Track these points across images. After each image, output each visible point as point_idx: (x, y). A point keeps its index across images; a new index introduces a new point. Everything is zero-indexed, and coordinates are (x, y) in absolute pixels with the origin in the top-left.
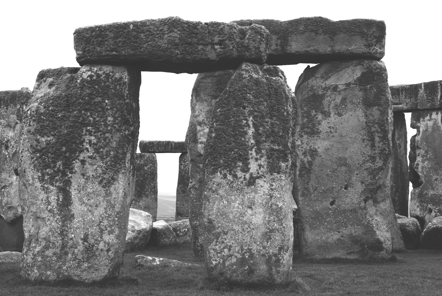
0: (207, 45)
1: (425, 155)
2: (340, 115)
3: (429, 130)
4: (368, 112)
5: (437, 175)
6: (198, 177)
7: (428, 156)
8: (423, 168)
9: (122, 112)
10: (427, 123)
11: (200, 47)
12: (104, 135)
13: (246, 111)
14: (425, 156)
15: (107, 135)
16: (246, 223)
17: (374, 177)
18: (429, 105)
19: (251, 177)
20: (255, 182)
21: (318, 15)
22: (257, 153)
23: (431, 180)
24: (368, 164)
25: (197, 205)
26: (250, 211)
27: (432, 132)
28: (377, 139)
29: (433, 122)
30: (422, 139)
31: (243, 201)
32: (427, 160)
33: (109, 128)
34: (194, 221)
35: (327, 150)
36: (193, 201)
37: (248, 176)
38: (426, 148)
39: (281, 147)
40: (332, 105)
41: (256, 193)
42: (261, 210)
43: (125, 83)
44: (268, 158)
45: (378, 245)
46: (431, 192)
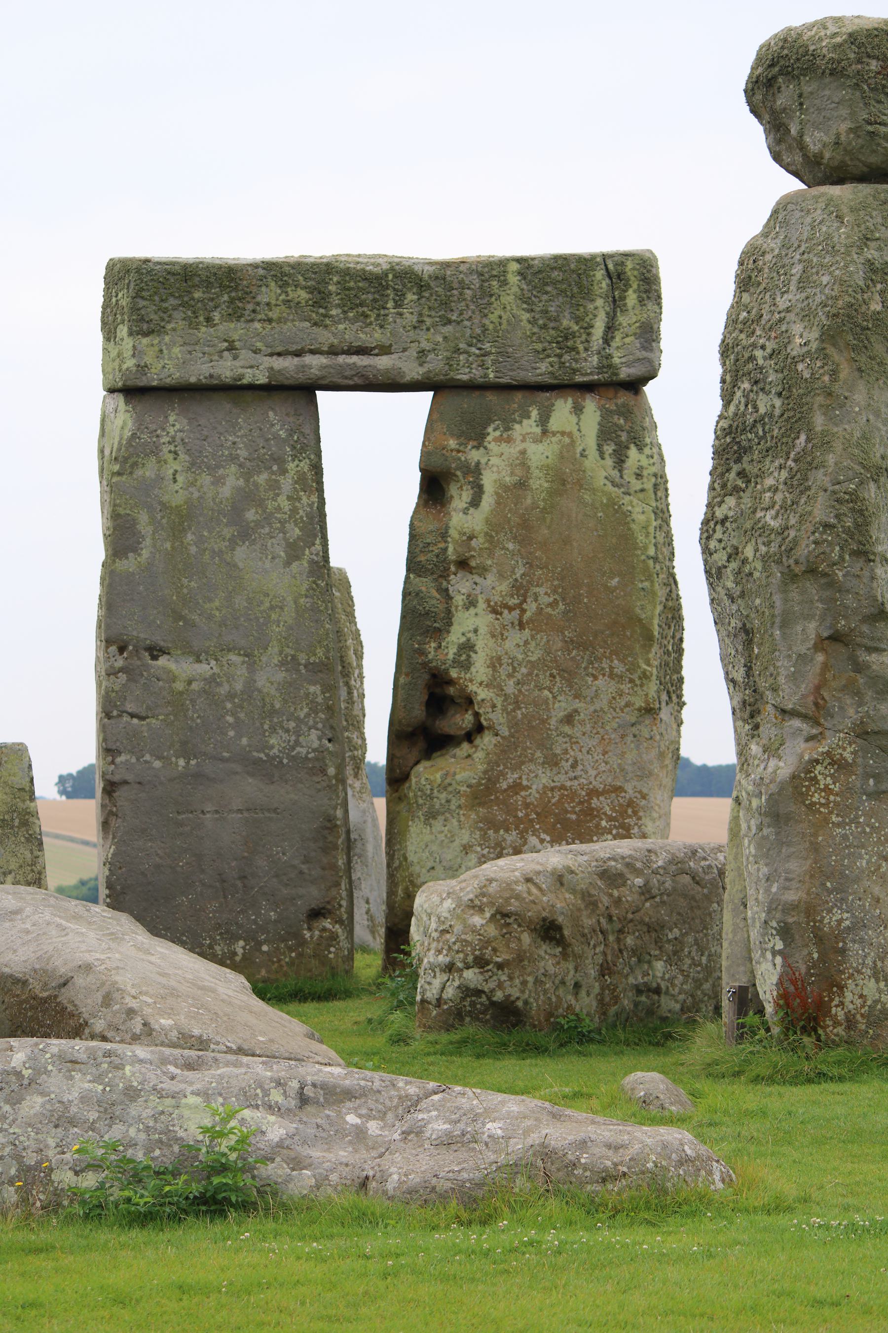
1: (515, 601)
3: (534, 484)
5: (577, 696)
6: (851, 712)
7: (531, 607)
8: (495, 663)
10: (523, 452)
14: (511, 609)
18: (543, 367)
23: (544, 721)
25: (845, 837)
27: (552, 493)
29: (556, 448)
30: (495, 526)
32: (522, 626)
34: (830, 911)
36: (826, 820)
38: (519, 572)
46: (539, 780)
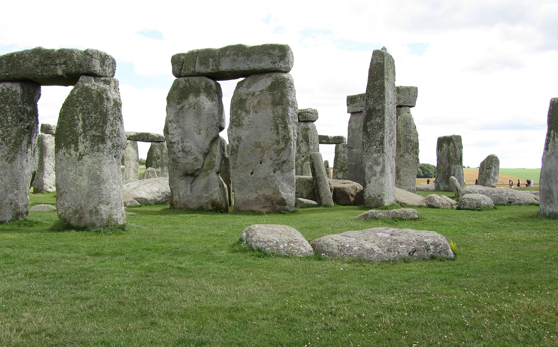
0: (57, 65)
2: (256, 112)
4: (275, 110)
9: (17, 113)
11: (52, 67)
12: (7, 128)
13: (78, 110)
15: (8, 129)
16: (78, 186)
17: (279, 155)
19: (80, 155)
20: (82, 158)
21: (239, 43)
22: (84, 138)
24: (275, 146)
26: (80, 177)
28: (280, 129)
31: (76, 171)
33: (10, 124)
35: (248, 137)
37: (78, 154)
39: (100, 134)
40: (251, 106)
41: (83, 166)
42: (86, 177)
43: (18, 94)
44: (92, 141)
45: (283, 202)
